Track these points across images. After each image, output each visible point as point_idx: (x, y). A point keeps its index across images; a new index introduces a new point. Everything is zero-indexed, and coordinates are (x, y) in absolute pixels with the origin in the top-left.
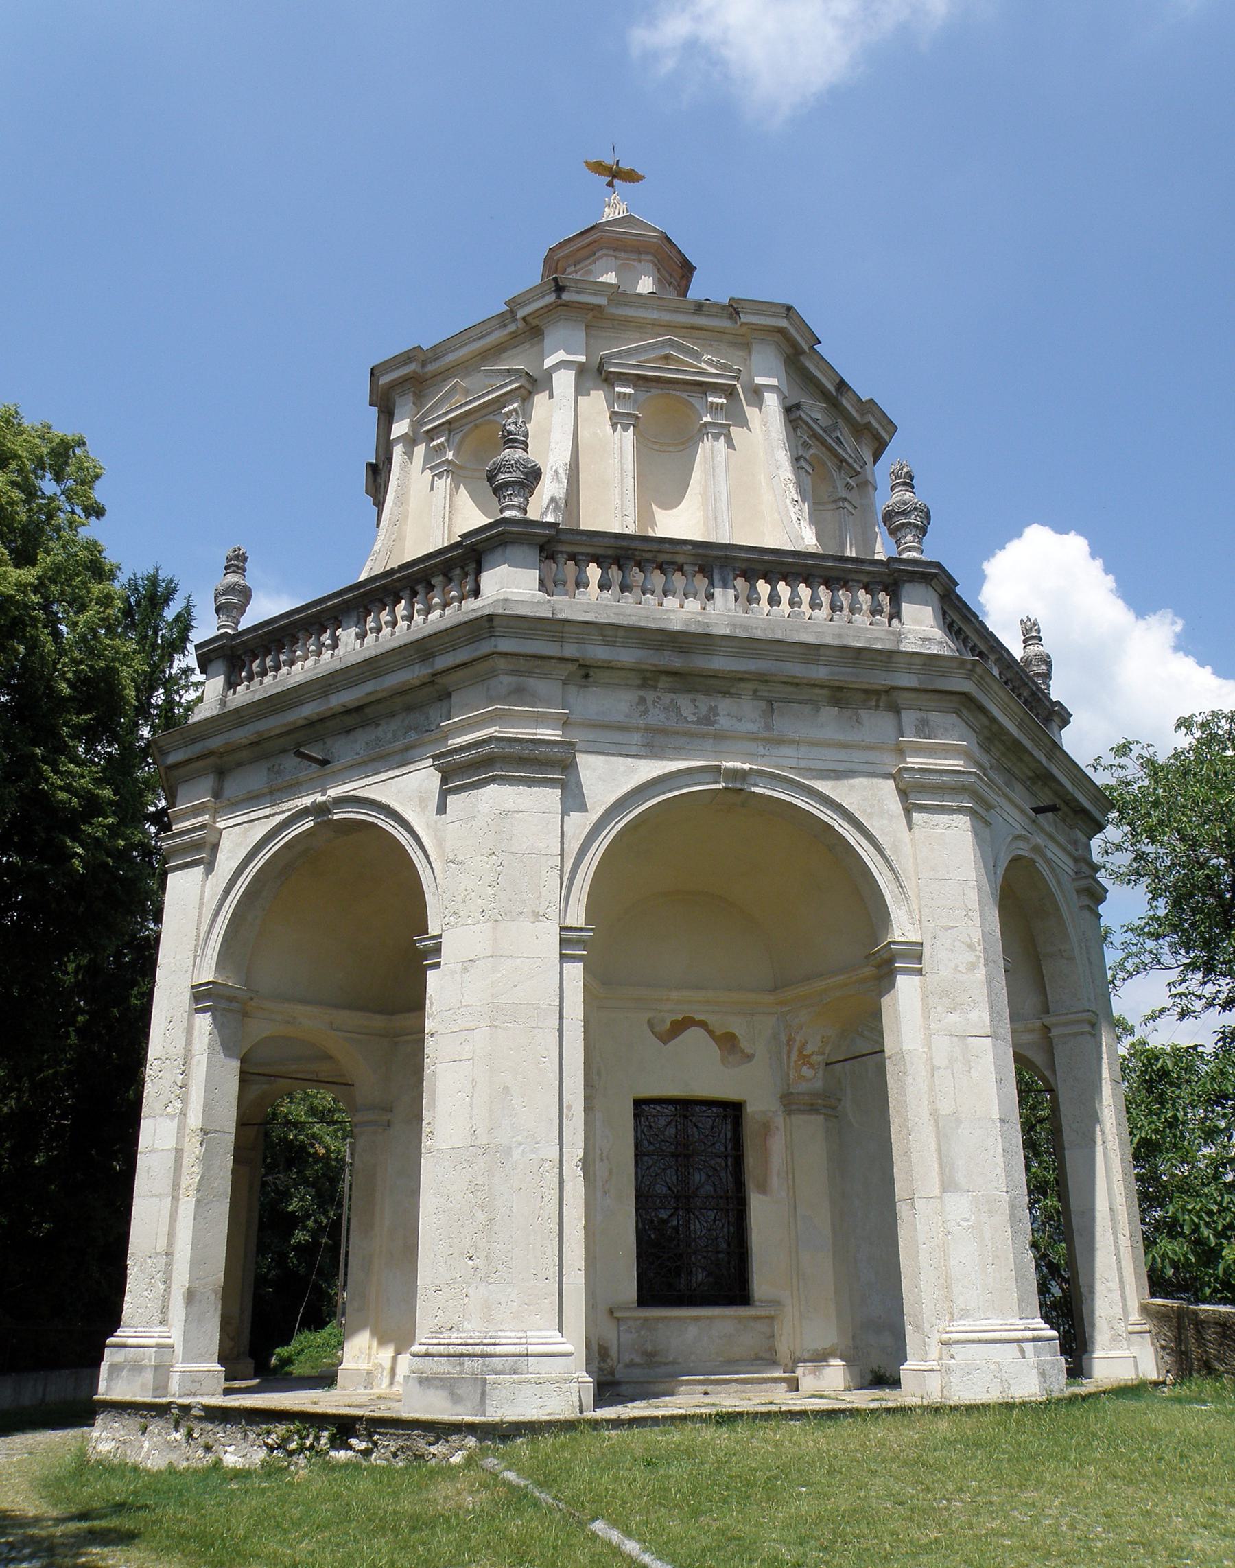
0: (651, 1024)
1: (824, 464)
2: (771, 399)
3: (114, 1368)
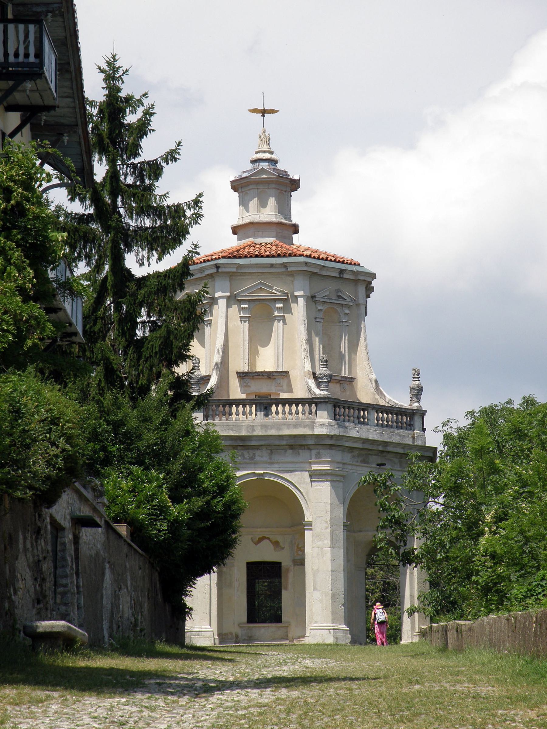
1: (334, 308)
2: (301, 301)
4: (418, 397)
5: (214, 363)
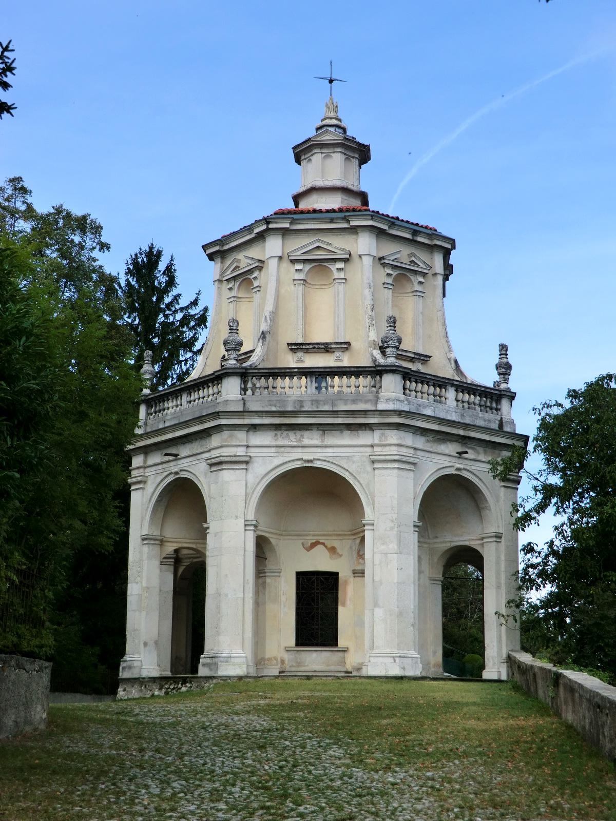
0: (303, 544)
3: (124, 668)
4: (506, 377)
5: (261, 333)
